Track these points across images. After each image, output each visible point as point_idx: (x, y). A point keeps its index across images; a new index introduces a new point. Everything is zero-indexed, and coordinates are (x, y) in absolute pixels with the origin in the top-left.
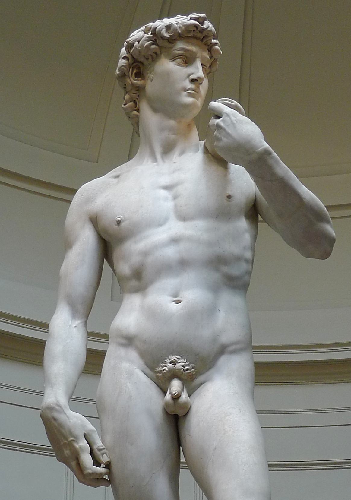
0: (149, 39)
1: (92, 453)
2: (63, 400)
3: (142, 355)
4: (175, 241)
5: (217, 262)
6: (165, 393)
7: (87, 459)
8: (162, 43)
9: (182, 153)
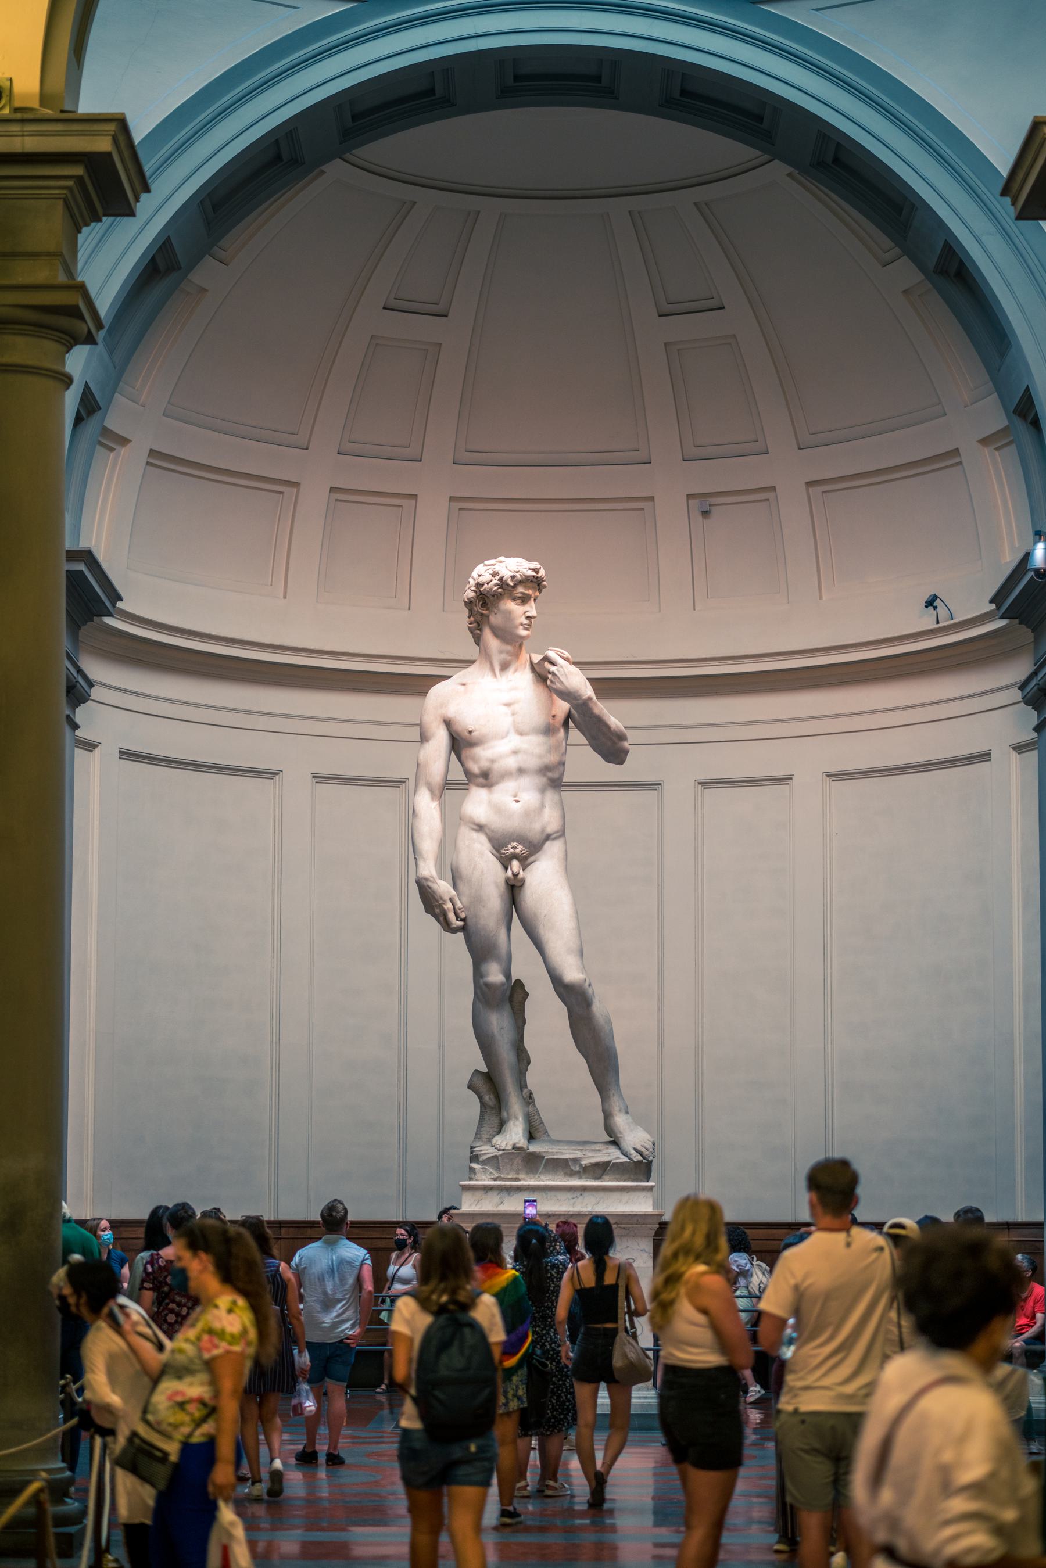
0: (497, 585)
1: (455, 913)
2: (434, 873)
3: (490, 839)
4: (515, 752)
5: (544, 770)
6: (506, 869)
7: (451, 916)
8: (506, 588)
9: (516, 671)
